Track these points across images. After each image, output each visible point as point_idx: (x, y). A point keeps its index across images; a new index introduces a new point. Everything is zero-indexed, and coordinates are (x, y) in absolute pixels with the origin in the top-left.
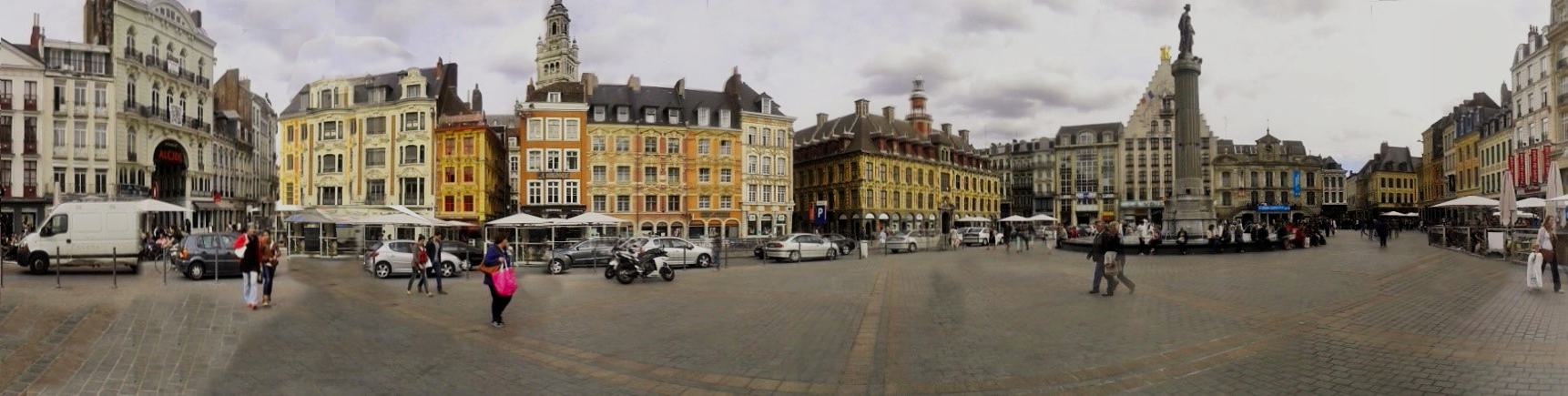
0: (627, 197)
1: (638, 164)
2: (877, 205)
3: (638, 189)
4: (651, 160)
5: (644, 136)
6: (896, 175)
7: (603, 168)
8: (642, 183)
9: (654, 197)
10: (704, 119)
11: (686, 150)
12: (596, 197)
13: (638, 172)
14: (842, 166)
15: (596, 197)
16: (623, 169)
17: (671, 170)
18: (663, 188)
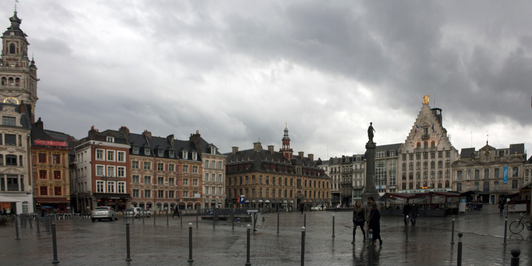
0: (149, 191)
1: (155, 175)
2: (264, 195)
3: (155, 187)
4: (161, 174)
5: (157, 163)
6: (274, 181)
7: (138, 177)
8: (157, 185)
9: (162, 191)
10: (185, 155)
11: (177, 170)
12: (134, 190)
13: (155, 180)
14: (247, 177)
15: (134, 190)
16: (148, 178)
17: (170, 179)
18: (166, 187)
